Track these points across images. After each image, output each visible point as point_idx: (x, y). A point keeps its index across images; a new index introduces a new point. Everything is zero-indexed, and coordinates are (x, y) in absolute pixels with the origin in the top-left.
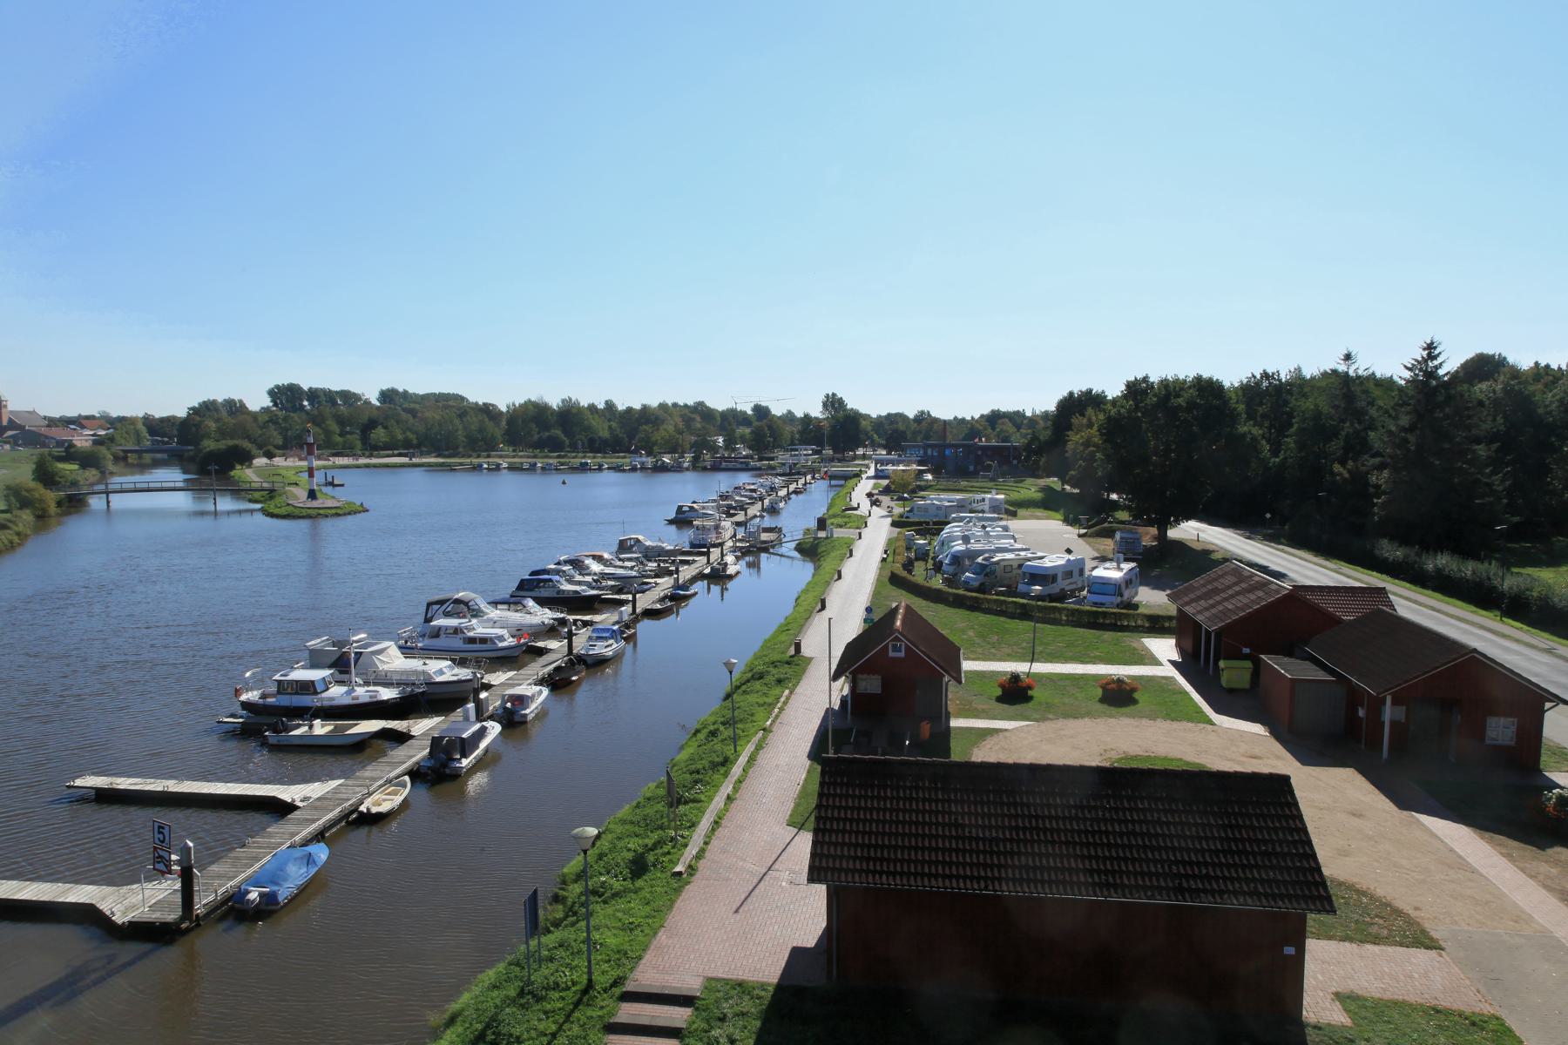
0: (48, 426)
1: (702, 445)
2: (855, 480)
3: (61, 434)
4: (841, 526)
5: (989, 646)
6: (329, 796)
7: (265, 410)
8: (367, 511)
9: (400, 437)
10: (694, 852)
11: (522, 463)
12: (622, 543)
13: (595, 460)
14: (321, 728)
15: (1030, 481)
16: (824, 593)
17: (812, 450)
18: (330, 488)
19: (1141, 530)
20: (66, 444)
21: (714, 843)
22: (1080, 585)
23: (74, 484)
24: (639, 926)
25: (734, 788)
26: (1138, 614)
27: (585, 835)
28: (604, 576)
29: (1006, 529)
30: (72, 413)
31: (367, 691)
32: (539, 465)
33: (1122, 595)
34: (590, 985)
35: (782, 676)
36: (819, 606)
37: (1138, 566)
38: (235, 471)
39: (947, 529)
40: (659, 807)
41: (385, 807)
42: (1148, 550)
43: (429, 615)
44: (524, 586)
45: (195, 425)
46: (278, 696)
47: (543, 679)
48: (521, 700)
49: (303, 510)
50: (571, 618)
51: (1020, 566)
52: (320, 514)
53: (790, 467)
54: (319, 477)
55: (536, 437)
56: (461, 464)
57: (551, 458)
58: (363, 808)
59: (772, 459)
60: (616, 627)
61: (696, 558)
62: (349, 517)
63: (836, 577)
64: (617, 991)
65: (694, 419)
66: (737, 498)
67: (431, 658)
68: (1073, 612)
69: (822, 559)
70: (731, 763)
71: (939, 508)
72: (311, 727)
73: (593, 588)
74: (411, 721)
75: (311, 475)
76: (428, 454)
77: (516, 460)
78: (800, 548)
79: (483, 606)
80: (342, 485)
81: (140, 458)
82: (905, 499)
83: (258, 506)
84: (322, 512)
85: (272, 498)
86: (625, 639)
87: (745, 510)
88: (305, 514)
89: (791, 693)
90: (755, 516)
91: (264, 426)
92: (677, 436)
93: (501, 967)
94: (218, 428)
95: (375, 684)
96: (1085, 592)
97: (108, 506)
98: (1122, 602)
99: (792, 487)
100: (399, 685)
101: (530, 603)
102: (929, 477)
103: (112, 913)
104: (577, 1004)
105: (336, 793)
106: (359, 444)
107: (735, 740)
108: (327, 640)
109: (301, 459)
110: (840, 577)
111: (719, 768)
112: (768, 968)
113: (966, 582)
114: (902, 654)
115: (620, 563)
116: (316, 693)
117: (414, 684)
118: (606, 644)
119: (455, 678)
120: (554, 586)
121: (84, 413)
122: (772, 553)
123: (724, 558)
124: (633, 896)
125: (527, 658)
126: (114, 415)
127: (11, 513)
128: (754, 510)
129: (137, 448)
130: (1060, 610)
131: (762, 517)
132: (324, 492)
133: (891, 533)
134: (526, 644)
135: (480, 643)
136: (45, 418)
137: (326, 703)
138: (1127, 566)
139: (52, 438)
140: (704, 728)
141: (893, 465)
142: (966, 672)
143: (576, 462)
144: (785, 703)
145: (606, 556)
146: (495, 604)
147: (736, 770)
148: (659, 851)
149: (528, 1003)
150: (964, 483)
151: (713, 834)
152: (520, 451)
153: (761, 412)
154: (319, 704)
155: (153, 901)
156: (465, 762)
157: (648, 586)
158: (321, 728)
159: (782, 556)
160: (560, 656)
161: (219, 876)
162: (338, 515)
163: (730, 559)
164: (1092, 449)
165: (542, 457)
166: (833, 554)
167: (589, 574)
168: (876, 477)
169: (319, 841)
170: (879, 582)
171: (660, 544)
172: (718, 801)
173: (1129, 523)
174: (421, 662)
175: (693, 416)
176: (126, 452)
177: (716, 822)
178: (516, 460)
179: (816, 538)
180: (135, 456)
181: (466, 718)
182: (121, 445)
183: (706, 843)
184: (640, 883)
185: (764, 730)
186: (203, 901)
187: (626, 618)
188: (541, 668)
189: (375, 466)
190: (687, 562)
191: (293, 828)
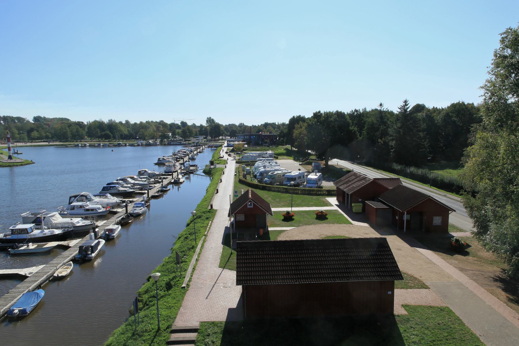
1: (164, 137)
2: (220, 147)
4: (218, 164)
5: (276, 203)
6: (40, 271)
8: (34, 163)
10: (188, 279)
11: (95, 144)
12: (140, 172)
13: (123, 142)
14: (32, 246)
15: (280, 147)
16: (216, 187)
17: (204, 137)
18: (17, 155)
19: (320, 162)
21: (194, 276)
22: (303, 181)
24: (173, 307)
25: (198, 256)
26: (324, 190)
27: (156, 276)
28: (134, 184)
29: (276, 163)
31: (49, 231)
32: (102, 144)
33: (318, 184)
34: (159, 329)
35: (208, 217)
36: (216, 192)
37: (322, 174)
39: (256, 164)
40: (172, 265)
41: (64, 274)
42: (323, 169)
43: (70, 202)
44: (104, 189)
46: (12, 235)
47: (118, 222)
48: (112, 231)
49: (7, 164)
50: (127, 200)
51: (284, 175)
52: (14, 165)
53: (197, 143)
54: (12, 151)
55: (99, 134)
56: (70, 145)
57: (106, 142)
58: (55, 275)
59: (189, 141)
60: (143, 202)
61: (168, 177)
63: (220, 181)
64: (169, 330)
65: (160, 127)
66: (179, 155)
67: (73, 217)
68: (302, 190)
70: (195, 248)
71: (252, 156)
72: (28, 246)
73: (131, 189)
74: (69, 241)
75: (9, 150)
76: (56, 141)
77: (92, 143)
78: (204, 172)
79: (93, 198)
80: (22, 154)
82: (239, 154)
84: (15, 164)
86: (146, 206)
87: (183, 159)
89: (212, 222)
90: (186, 161)
92: (154, 133)
93: (123, 326)
95: (52, 228)
96: (305, 183)
98: (318, 186)
99: (198, 150)
100: (62, 228)
101: (109, 195)
102: (246, 146)
104: (155, 336)
105: (42, 270)
106: (26, 137)
107: (195, 240)
108: (29, 213)
110: (221, 181)
111: (191, 250)
112: (222, 317)
113: (266, 182)
114: (252, 207)
115: (141, 179)
116: (28, 233)
117: (68, 227)
118: (140, 209)
119: (84, 224)
120: (117, 189)
122: (195, 174)
123: (179, 176)
124: (169, 297)
125: (110, 215)
128: (186, 159)
130: (299, 190)
131: (189, 161)
133: (236, 165)
134: (109, 210)
135: (91, 211)
137: (32, 237)
138: (318, 174)
140: (182, 236)
141: (233, 142)
142: (274, 212)
143: (116, 143)
144: (211, 226)
145: (135, 177)
146: (95, 196)
147: (198, 250)
148: (175, 280)
149: (137, 338)
150: (258, 148)
151: (193, 273)
152: (93, 139)
153: (184, 124)
154: (29, 237)
156: (93, 255)
157: (152, 187)
158: (32, 246)
159: (198, 175)
160: (123, 214)
162: (22, 165)
163: (180, 176)
164: (302, 135)
165: (102, 142)
166: (217, 174)
167: (128, 184)
168: (227, 146)
170: (235, 182)
171: (154, 172)
172: (193, 261)
173: (315, 160)
174: (70, 219)
175: (160, 126)
177: (194, 269)
178: (92, 143)
179: (210, 168)
181: (91, 239)
183: (191, 276)
184: (170, 292)
185: (205, 235)
187: (146, 199)
188: (116, 219)
189: (34, 146)
190: (164, 178)
191: (28, 285)
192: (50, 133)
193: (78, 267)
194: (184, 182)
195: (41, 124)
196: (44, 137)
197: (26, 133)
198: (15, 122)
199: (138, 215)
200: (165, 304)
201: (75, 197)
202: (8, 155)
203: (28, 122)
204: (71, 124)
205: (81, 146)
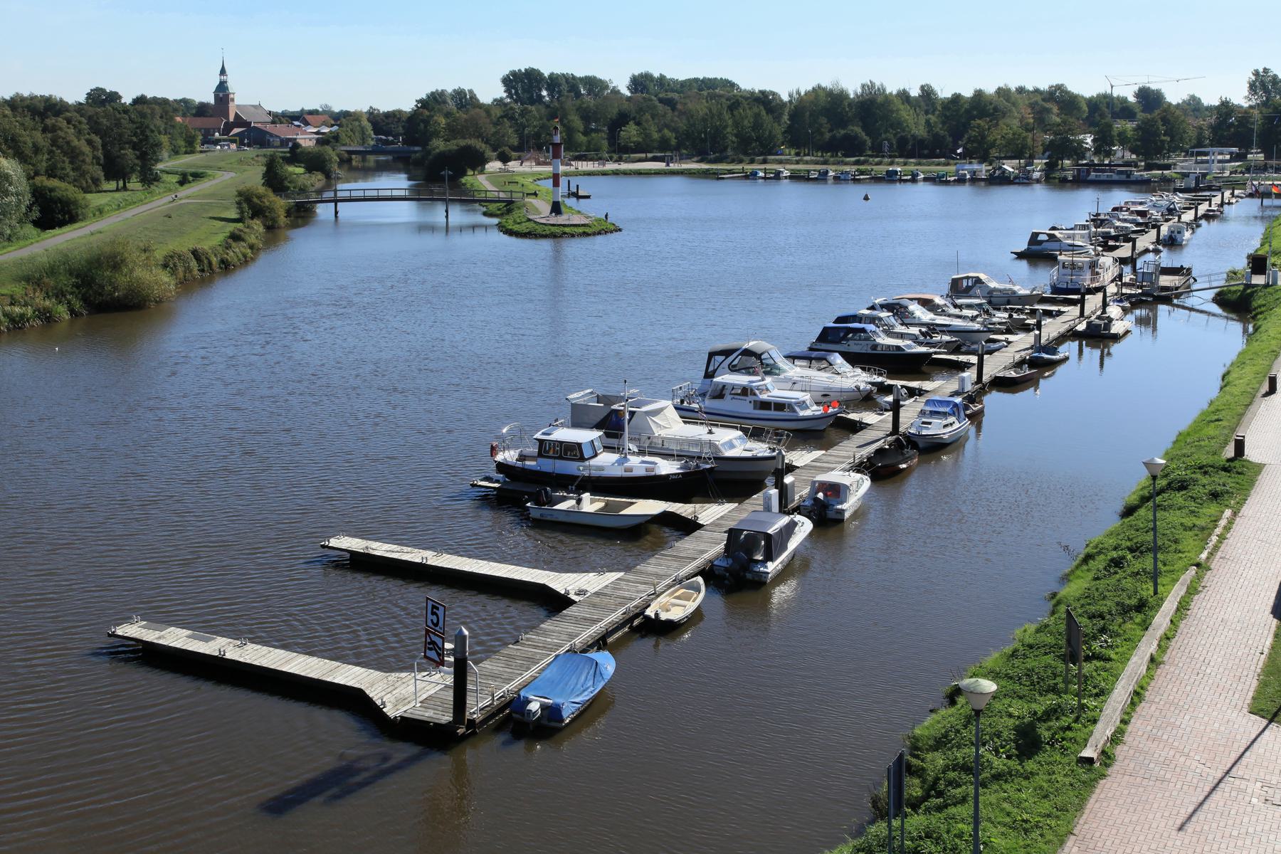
0: (273, 122)
1: (1061, 148)
3: (283, 131)
6: (608, 591)
7: (499, 102)
8: (620, 230)
9: (656, 136)
10: (1109, 733)
11: (808, 171)
12: (955, 284)
13: (906, 168)
14: (591, 504)
16: (1270, 367)
17: (1231, 154)
20: (290, 144)
21: (1136, 724)
23: (303, 190)
24: (1037, 827)
25: (1159, 646)
28: (932, 329)
30: (294, 107)
32: (831, 173)
35: (1219, 489)
36: (1265, 387)
40: (1049, 659)
41: (676, 614)
43: (711, 369)
44: (827, 336)
45: (423, 121)
46: (539, 459)
47: (861, 463)
48: (836, 491)
49: (546, 228)
50: (899, 383)
52: (565, 233)
53: (1197, 179)
55: (828, 136)
56: (730, 172)
57: (846, 164)
58: (650, 612)
59: (1168, 167)
60: (958, 400)
61: (1063, 309)
62: (599, 238)
65: (1049, 111)
66: (1118, 224)
67: (717, 425)
69: (1259, 316)
70: (1151, 608)
72: (579, 501)
73: (921, 344)
74: (698, 506)
75: (556, 184)
76: (688, 158)
78: (1222, 299)
79: (783, 363)
80: (588, 197)
81: (364, 160)
83: (495, 221)
84: (567, 230)
85: (509, 211)
86: (970, 417)
87: (1134, 241)
88: (548, 232)
89: (1235, 514)
90: (1147, 251)
92: (1025, 134)
94: (448, 124)
95: (651, 454)
97: (336, 216)
99: (1203, 208)
100: (679, 457)
101: (838, 360)
103: (383, 703)
105: (615, 589)
106: (605, 143)
107: (1155, 576)
108: (592, 393)
109: (538, 164)
111: (1133, 614)
115: (957, 311)
116: (582, 459)
117: (699, 458)
118: (945, 422)
119: (749, 454)
120: (868, 339)
121: (307, 108)
122: (1178, 306)
123: (1108, 309)
124: (1024, 783)
125: (833, 433)
126: (337, 109)
127: (243, 223)
128: (1145, 241)
129: (362, 149)
131: (1157, 252)
132: (568, 205)
134: (835, 414)
135: (775, 410)
136: (270, 113)
137: (594, 473)
139: (277, 136)
140: (1100, 553)
143: (882, 169)
144: (1227, 528)
145: (938, 300)
146: (792, 358)
147: (1161, 620)
148: (1054, 724)
151: (1134, 710)
152: (805, 155)
153: (1149, 98)
154: (586, 473)
155: (424, 696)
156: (772, 567)
157: (997, 345)
158: (591, 504)
159: (1191, 309)
160: (881, 434)
161: (494, 677)
162: (586, 234)
163: (1114, 311)
165: (834, 164)
167: (912, 325)
169: (599, 649)
171: (1008, 286)
172: (1137, 663)
174: (706, 429)
175: (1048, 105)
176: (350, 153)
177: (1136, 693)
179: (1248, 286)
180: (359, 158)
181: (768, 508)
182: (344, 145)
183: (1124, 722)
184: (1030, 765)
185: (1198, 565)
186: (476, 706)
187: (969, 387)
188: (853, 448)
190: (1048, 314)
191: (572, 628)
192: (674, 130)
193: (718, 600)
194: (1129, 336)
195: (651, 100)
196: (656, 144)
197: (605, 129)
198: (578, 95)
199: (934, 448)
200: (1005, 805)
201: (727, 353)
202: (552, 201)
203: (615, 92)
204: (738, 100)
205: (765, 178)
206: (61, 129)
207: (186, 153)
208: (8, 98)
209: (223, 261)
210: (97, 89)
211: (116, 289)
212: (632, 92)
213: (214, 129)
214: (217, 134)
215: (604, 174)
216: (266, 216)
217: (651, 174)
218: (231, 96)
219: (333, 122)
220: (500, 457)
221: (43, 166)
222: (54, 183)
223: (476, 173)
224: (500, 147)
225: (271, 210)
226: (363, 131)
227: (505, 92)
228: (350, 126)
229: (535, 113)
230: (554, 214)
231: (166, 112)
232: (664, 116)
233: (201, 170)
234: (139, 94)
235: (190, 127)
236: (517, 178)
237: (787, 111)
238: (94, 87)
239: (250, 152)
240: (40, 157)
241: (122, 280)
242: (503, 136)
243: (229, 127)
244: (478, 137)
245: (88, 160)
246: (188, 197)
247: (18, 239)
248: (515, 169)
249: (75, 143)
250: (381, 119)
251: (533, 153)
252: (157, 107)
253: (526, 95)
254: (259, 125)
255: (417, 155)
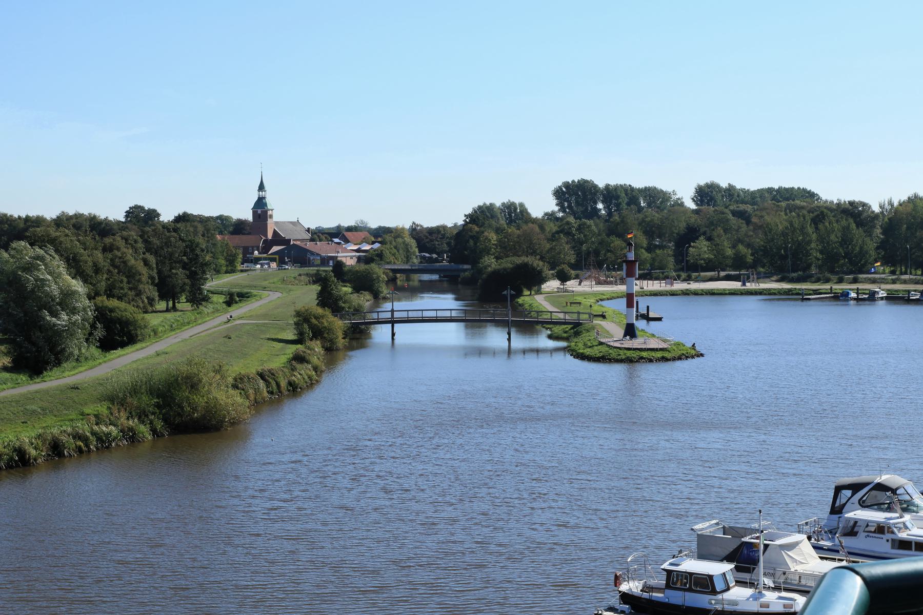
0: (312, 240)
3: (323, 249)
7: (550, 216)
8: (702, 355)
9: (729, 252)
11: (909, 291)
18: (645, 322)
30: (329, 223)
31: (780, 598)
38: (522, 298)
43: (837, 504)
45: (472, 237)
46: (666, 591)
49: (621, 352)
52: (642, 358)
56: (816, 292)
76: (767, 276)
77: (897, 287)
80: (659, 319)
84: (644, 354)
85: (577, 334)
88: (624, 357)
91: (553, 238)
94: (499, 241)
95: (787, 590)
109: (599, 283)
116: (714, 592)
121: (346, 224)
126: (374, 225)
129: (407, 267)
136: (308, 230)
137: (728, 608)
139: (318, 254)
152: (902, 274)
162: (664, 359)
178: (897, 287)
182: (389, 263)
189: (696, 293)
192: (748, 246)
195: (723, 213)
196: (729, 262)
197: (671, 244)
201: (855, 487)
202: (625, 322)
203: (679, 204)
204: (822, 212)
205: (857, 299)
206: (118, 249)
207: (227, 272)
208: (54, 217)
209: (290, 384)
210: (137, 207)
211: (195, 409)
212: (697, 205)
213: (253, 247)
214: (256, 252)
215: (673, 294)
216: (325, 338)
217: (726, 294)
218: (270, 213)
219: (373, 239)
220: (624, 587)
221: (103, 285)
222: (114, 303)
223: (533, 293)
224: (559, 266)
225: (330, 330)
226: (407, 249)
227: (557, 205)
228: (394, 243)
229: (594, 227)
230: (628, 337)
231: (208, 230)
232: (737, 231)
233: (245, 290)
234: (181, 212)
235: (231, 245)
236: (577, 298)
237: (878, 223)
238: (132, 205)
239: (291, 270)
240: (99, 277)
241: (200, 401)
242: (560, 253)
243: (268, 245)
244: (532, 254)
245: (144, 278)
246: (241, 318)
247: (86, 359)
248: (574, 289)
249: (133, 262)
250: (425, 236)
251: (594, 272)
252: (199, 225)
253: (581, 209)
254: (298, 243)
255: (466, 273)
